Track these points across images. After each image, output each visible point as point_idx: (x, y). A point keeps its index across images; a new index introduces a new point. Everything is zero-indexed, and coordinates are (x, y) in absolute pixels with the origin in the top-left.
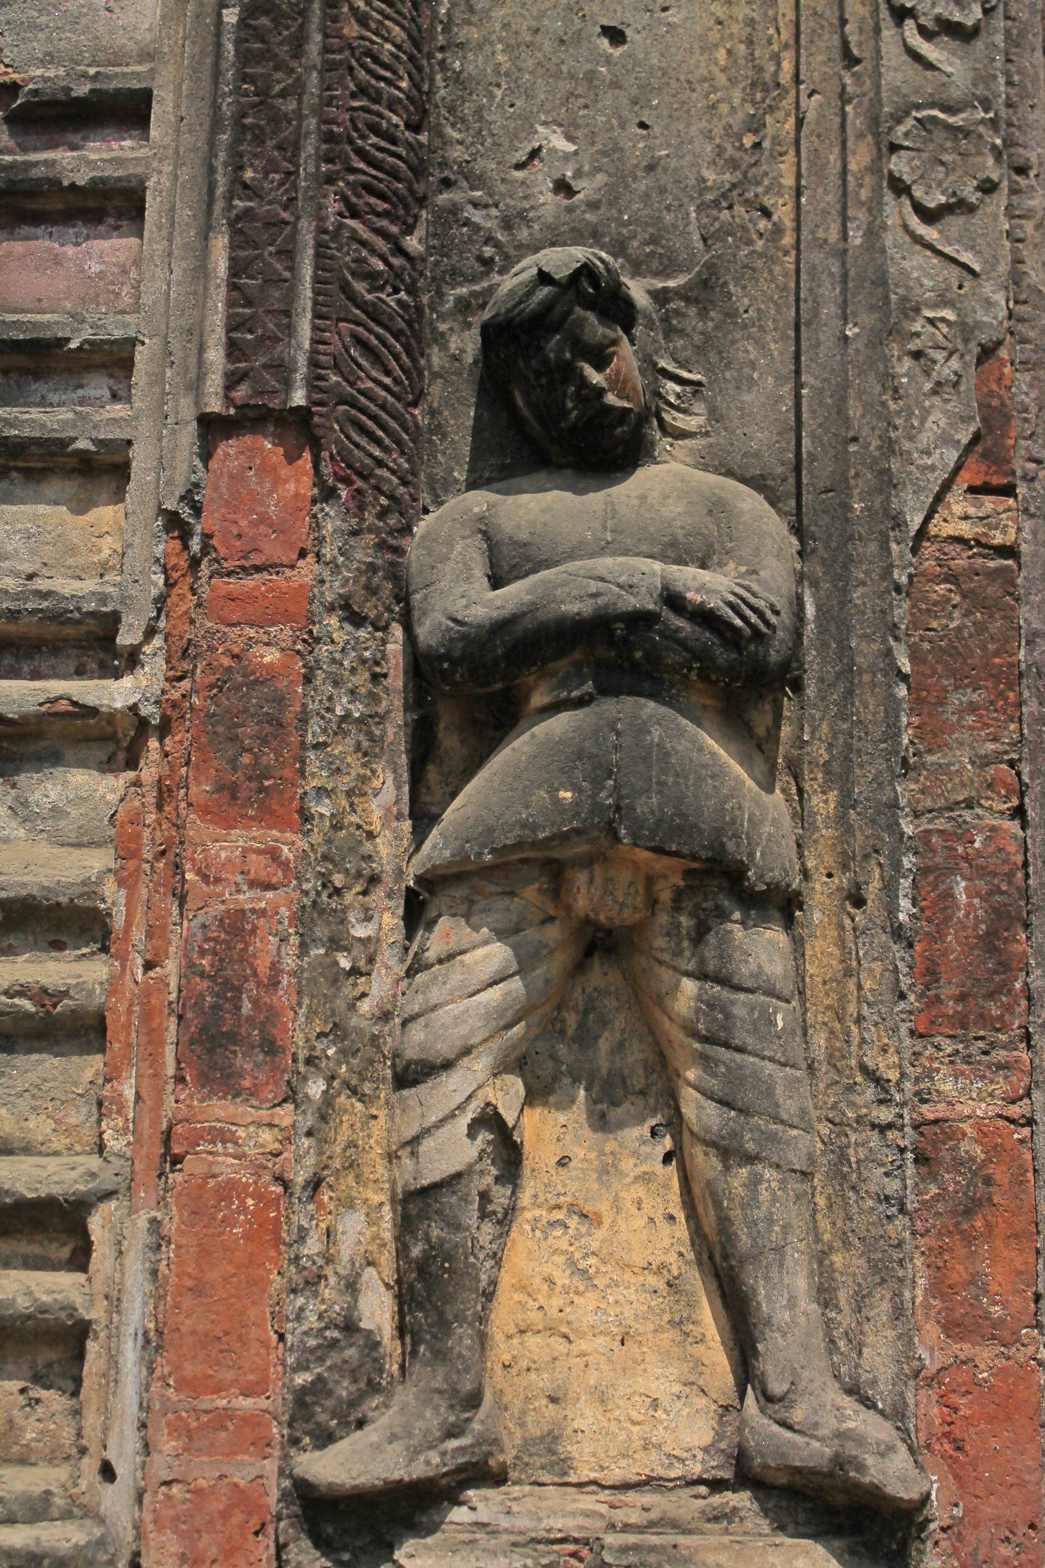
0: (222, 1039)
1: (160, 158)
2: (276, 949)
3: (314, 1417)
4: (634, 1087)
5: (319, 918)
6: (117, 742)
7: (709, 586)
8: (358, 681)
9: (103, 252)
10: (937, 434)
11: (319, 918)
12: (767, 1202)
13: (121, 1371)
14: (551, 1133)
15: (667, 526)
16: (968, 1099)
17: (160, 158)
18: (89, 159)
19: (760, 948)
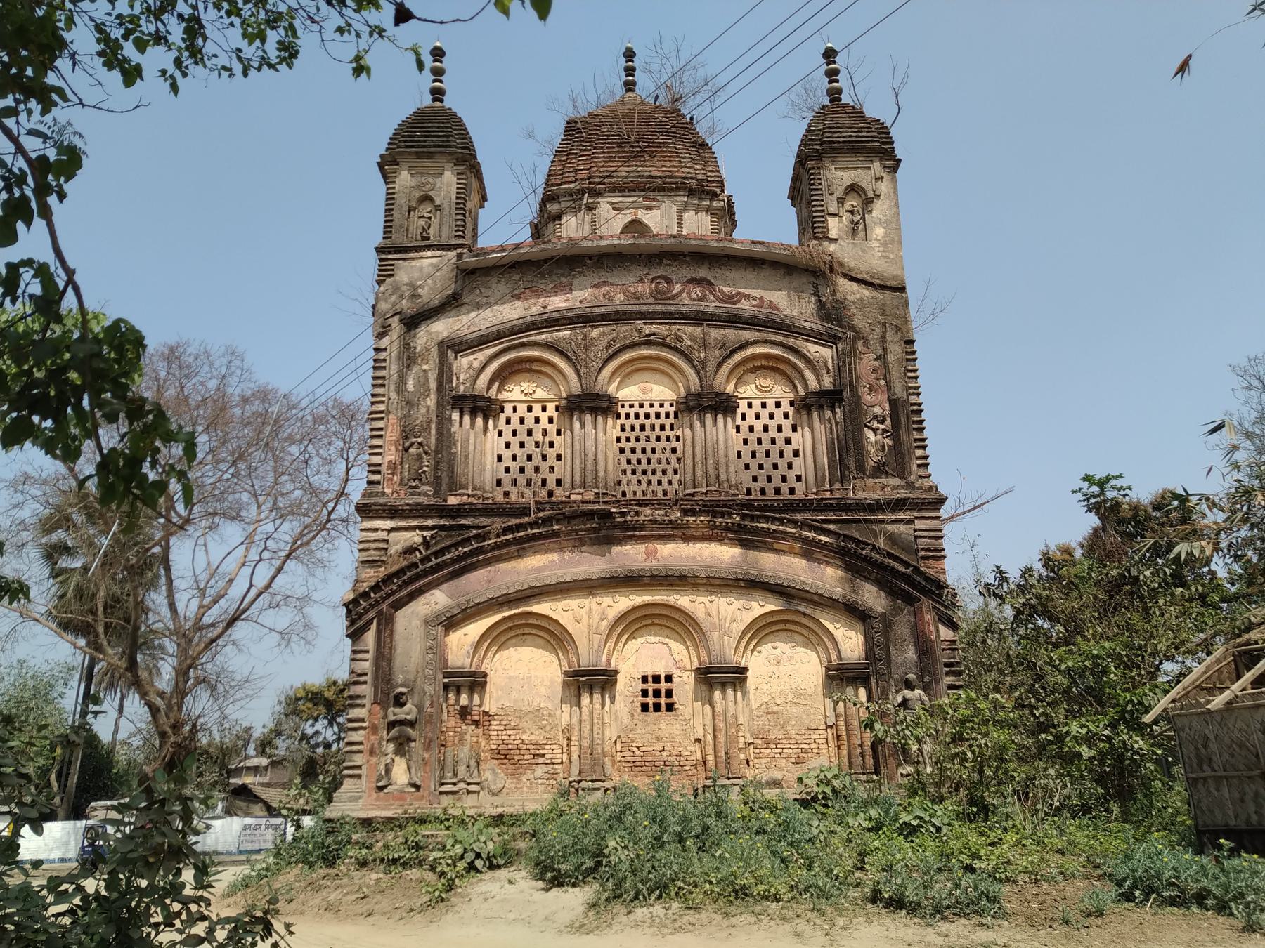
0: (372, 752)
1: (368, 678)
2: (376, 746)
3: (378, 781)
4: (403, 755)
5: (380, 743)
6: (364, 728)
7: (409, 717)
8: (382, 724)
9: (364, 687)
10: (428, 703)
11: (380, 743)
12: (412, 763)
13: (364, 778)
14: (397, 759)
15: (408, 711)
16: (426, 756)
17: (368, 678)
18: (362, 679)
19: (412, 744)
